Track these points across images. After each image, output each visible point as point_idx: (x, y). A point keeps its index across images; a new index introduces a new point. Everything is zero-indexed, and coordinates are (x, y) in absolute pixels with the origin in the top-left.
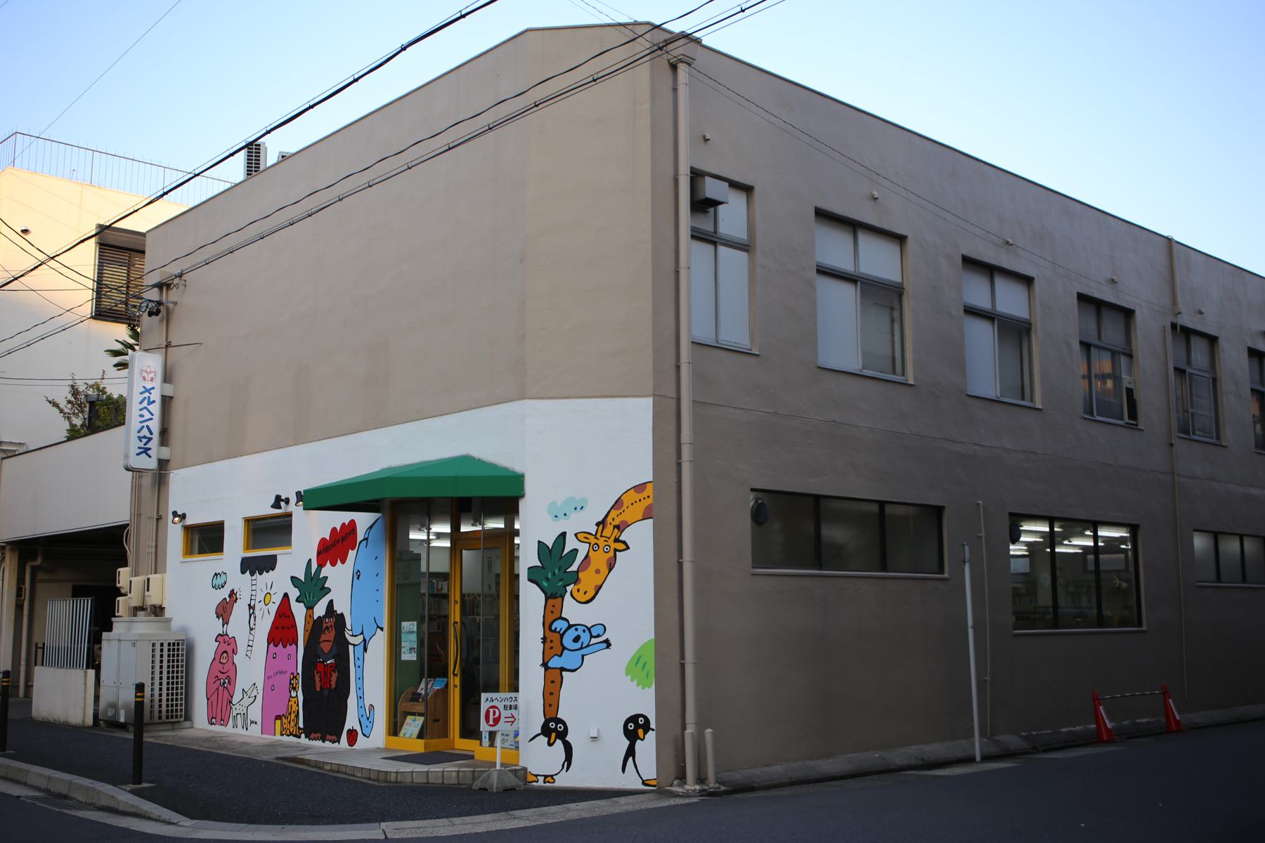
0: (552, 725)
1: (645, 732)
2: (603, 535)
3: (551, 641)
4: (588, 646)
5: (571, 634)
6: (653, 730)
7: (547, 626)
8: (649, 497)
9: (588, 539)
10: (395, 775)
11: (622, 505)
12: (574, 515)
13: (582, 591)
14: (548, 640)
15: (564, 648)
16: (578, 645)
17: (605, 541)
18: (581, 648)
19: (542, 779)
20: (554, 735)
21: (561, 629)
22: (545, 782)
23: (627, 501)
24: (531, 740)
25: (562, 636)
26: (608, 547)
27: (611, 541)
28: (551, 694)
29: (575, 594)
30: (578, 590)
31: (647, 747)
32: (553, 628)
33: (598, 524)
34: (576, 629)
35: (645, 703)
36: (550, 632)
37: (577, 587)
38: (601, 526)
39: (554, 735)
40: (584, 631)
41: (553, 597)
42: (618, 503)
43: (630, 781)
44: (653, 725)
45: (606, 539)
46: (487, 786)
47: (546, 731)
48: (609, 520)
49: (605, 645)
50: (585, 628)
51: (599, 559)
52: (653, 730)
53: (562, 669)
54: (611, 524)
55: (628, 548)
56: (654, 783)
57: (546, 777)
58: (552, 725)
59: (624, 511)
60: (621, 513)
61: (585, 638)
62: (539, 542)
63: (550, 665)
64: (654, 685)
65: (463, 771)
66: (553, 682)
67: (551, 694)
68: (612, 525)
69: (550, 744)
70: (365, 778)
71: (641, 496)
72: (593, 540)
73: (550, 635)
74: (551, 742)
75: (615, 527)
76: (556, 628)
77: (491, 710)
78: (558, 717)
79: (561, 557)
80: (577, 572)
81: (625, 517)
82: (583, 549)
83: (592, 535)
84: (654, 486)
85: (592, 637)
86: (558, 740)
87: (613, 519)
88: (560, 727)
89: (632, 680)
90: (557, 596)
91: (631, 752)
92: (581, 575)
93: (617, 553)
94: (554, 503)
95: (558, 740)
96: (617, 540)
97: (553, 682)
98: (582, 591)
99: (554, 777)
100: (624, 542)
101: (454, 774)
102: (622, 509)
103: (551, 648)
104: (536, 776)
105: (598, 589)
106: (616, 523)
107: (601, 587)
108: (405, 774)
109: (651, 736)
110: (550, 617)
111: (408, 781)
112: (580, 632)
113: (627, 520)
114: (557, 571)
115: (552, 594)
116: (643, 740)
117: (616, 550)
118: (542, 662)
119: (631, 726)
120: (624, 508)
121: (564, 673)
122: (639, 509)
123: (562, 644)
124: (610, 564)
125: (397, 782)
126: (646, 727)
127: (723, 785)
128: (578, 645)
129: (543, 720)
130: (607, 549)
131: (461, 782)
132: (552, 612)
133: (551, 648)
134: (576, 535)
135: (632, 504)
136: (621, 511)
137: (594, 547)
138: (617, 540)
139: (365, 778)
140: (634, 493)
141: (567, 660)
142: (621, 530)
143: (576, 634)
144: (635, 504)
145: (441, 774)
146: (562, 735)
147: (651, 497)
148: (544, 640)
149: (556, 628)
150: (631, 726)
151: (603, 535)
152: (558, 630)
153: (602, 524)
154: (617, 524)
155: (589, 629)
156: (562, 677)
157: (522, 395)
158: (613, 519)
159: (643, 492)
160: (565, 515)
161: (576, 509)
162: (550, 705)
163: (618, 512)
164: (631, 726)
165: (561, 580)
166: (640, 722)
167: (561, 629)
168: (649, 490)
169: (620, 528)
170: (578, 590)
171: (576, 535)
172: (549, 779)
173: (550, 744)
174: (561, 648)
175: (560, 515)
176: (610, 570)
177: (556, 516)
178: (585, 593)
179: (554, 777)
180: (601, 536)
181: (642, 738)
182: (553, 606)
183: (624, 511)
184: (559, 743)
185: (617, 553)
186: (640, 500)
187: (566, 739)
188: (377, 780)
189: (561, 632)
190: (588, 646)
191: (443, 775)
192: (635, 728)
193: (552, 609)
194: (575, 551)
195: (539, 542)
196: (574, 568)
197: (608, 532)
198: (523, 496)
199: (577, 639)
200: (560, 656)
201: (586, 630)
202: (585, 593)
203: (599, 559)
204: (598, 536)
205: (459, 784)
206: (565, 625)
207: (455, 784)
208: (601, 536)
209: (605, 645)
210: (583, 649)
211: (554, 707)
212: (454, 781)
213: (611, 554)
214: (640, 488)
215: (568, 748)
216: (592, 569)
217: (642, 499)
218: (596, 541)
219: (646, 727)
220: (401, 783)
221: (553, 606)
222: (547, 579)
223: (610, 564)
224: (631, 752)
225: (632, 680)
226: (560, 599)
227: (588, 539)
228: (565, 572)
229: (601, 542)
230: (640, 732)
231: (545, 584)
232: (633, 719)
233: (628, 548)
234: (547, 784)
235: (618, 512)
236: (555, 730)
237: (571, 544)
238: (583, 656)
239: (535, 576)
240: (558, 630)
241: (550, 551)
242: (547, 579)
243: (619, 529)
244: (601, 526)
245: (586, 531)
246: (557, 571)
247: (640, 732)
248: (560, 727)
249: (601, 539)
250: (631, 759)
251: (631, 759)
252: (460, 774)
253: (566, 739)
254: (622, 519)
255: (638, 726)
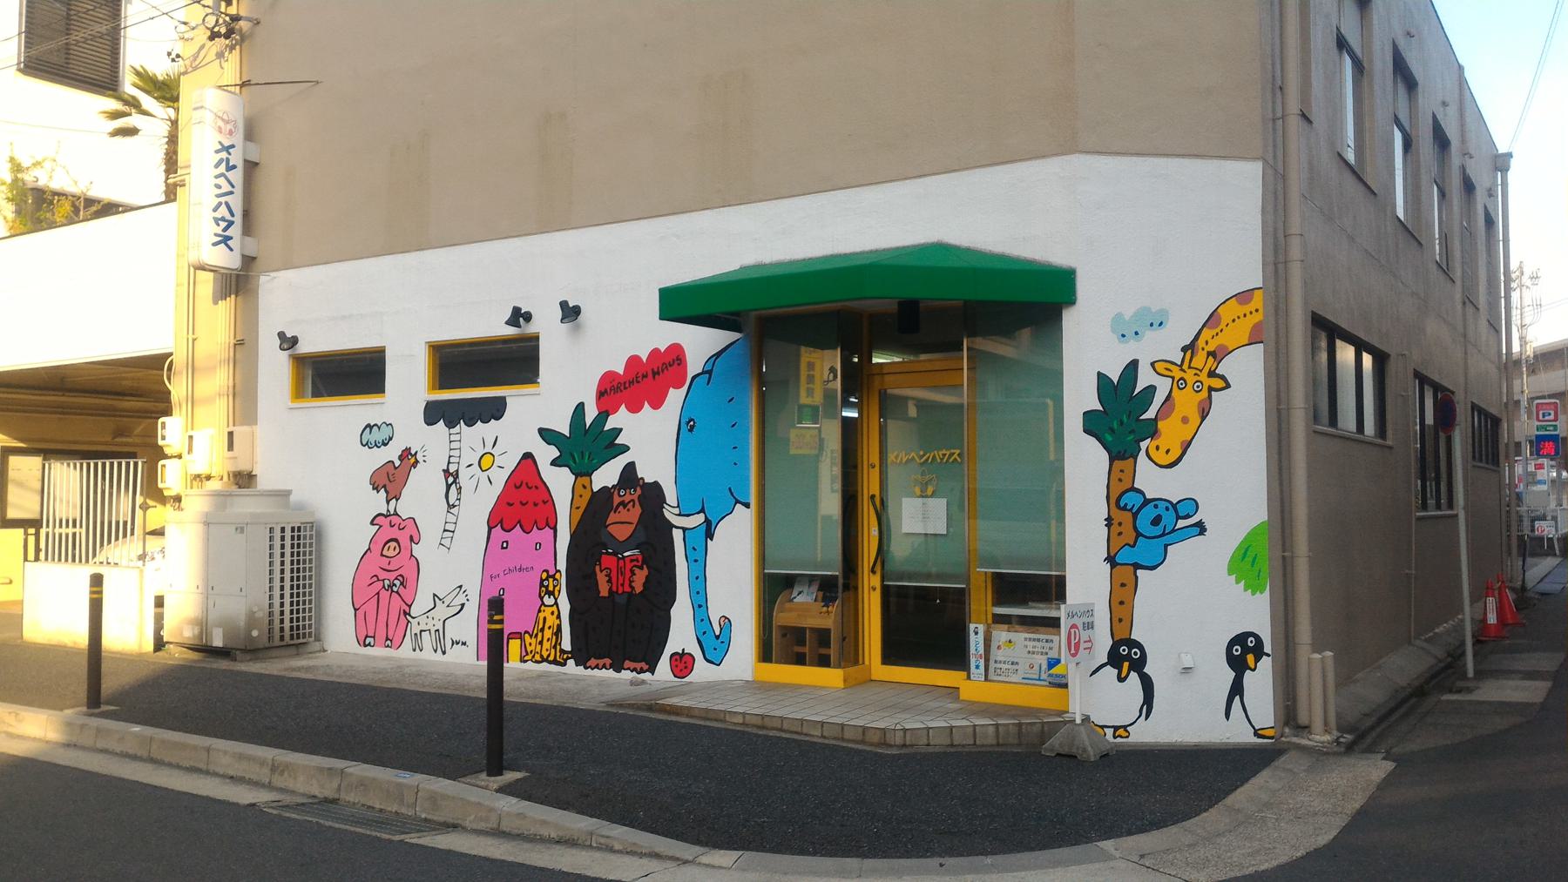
0: (1124, 650)
1: (1257, 660)
2: (1192, 365)
3: (1120, 524)
4: (1173, 531)
5: (1149, 513)
6: (1268, 655)
7: (1113, 501)
8: (1257, 311)
9: (1171, 371)
10: (902, 733)
11: (1219, 323)
12: (1149, 335)
13: (1163, 450)
14: (1115, 522)
15: (1139, 534)
16: (1158, 530)
17: (1195, 374)
18: (1163, 535)
19: (1109, 732)
20: (1126, 665)
21: (1134, 505)
22: (1115, 737)
23: (1226, 314)
24: (1094, 673)
25: (1135, 516)
26: (1199, 384)
27: (1203, 376)
28: (1122, 603)
29: (1152, 452)
30: (1157, 448)
31: (1261, 681)
32: (1122, 505)
33: (1184, 349)
34: (1156, 507)
35: (1256, 615)
36: (1118, 511)
37: (1155, 443)
38: (1189, 353)
39: (1126, 665)
40: (1167, 509)
41: (1121, 453)
42: (1213, 319)
43: (1237, 732)
44: (1268, 648)
45: (1198, 372)
46: (1074, 751)
47: (1114, 659)
48: (1201, 343)
49: (1197, 530)
50: (1168, 505)
51: (1187, 402)
52: (1268, 655)
53: (1137, 566)
54: (1203, 349)
55: (1228, 386)
56: (1270, 733)
57: (1116, 728)
58: (1124, 650)
59: (1221, 331)
60: (1217, 334)
61: (1169, 518)
62: (1099, 373)
63: (1119, 559)
64: (1268, 587)
65: (1004, 725)
66: (1123, 585)
67: (1122, 603)
68: (1205, 352)
69: (1121, 679)
70: (835, 738)
71: (1247, 309)
72: (1178, 374)
73: (1119, 516)
74: (1123, 676)
75: (1209, 354)
76: (1126, 504)
77: (1072, 631)
78: (1132, 637)
79: (1132, 398)
80: (1155, 420)
81: (1225, 339)
82: (1163, 387)
83: (1176, 364)
84: (1264, 293)
85: (1178, 518)
86: (1132, 672)
87: (1207, 343)
88: (1136, 654)
89: (1237, 582)
90: (1127, 455)
91: (1237, 689)
92: (1161, 424)
93: (1213, 393)
94: (1119, 316)
95: (1132, 672)
96: (1212, 374)
97: (1123, 585)
98: (1163, 450)
99: (1128, 728)
100: (1223, 378)
101: (991, 730)
102: (1218, 330)
103: (1120, 534)
104: (1102, 727)
105: (1186, 446)
106: (1211, 347)
107: (1190, 443)
108: (920, 732)
109: (1266, 663)
110: (1117, 490)
111: (921, 743)
112: (1161, 511)
113: (1226, 344)
114: (1125, 419)
115: (1119, 452)
116: (1254, 670)
117: (1211, 389)
118: (1106, 556)
119: (1237, 651)
120: (1222, 326)
121: (1139, 572)
122: (1243, 329)
123: (1135, 528)
124: (1203, 410)
125: (904, 745)
126: (1259, 652)
127: (1348, 733)
128: (1158, 530)
129: (1110, 642)
130: (1198, 387)
131: (1001, 741)
132: (1120, 480)
133: (1120, 534)
134: (1153, 364)
135: (1234, 321)
136: (1218, 330)
137: (1180, 383)
138: (1212, 374)
139: (835, 738)
140: (1235, 302)
141: (1142, 552)
142: (1219, 359)
143: (1157, 512)
144: (1231, 324)
145: (972, 729)
146: (1138, 665)
147: (1261, 311)
148: (1109, 521)
149: (1126, 504)
150: (1237, 650)
151: (1192, 365)
152: (1129, 507)
153: (1190, 348)
154: (1212, 350)
155: (1174, 506)
156: (1137, 577)
157: (1068, 146)
158: (1207, 343)
159: (1250, 302)
160: (1136, 333)
161: (1152, 325)
162: (1120, 620)
163: (1214, 332)
164: (1237, 650)
165: (1132, 432)
166: (1239, 648)
167: (1134, 505)
168: (1258, 297)
169: (1217, 355)
170: (1157, 448)
171: (1153, 364)
172: (1121, 732)
173: (1121, 679)
174: (1135, 534)
175: (1130, 334)
176: (1203, 418)
177: (1123, 336)
178: (1168, 452)
179: (1128, 728)
180: (1190, 367)
181: (1253, 667)
182: (1122, 471)
183: (1221, 331)
184: (1134, 676)
185: (1213, 393)
186: (1245, 315)
187: (1145, 670)
188: (863, 742)
189: (1134, 511)
190: (1173, 531)
191: (975, 730)
192: (1242, 652)
193: (1122, 476)
194: (1151, 389)
195: (1099, 373)
196: (1150, 414)
197: (1199, 360)
198: (1072, 302)
199: (1156, 521)
200: (1133, 546)
201: (1170, 507)
202: (1168, 452)
203: (1187, 402)
204: (1185, 367)
205: (998, 745)
206: (1139, 500)
207: (992, 745)
208: (1190, 367)
209: (1197, 530)
210: (1168, 536)
211: (1126, 623)
212: (991, 740)
213: (1204, 394)
214: (1244, 297)
215: (1147, 685)
216: (1175, 418)
217: (1254, 312)
218: (1182, 374)
219: (1259, 652)
220: (912, 746)
221: (1122, 471)
222: (1112, 430)
223: (1203, 410)
224: (1237, 689)
225: (1237, 582)
226: (1131, 460)
227: (1171, 371)
228: (1138, 420)
229: (1190, 376)
230: (1250, 658)
231: (1109, 438)
232: (1240, 639)
233: (1228, 386)
234: (1119, 740)
235: (1214, 332)
236: (1128, 657)
237: (1145, 378)
238: (1166, 546)
239: (1093, 424)
240: (1129, 507)
241: (1116, 388)
242: (1112, 430)
243: (1215, 357)
244: (1189, 353)
245: (1168, 359)
246: (1125, 419)
247: (1250, 658)
248: (1136, 654)
249: (1188, 371)
250: (1237, 698)
251: (1237, 698)
252: (1000, 729)
253: (1145, 670)
254: (1220, 342)
255: (1246, 650)
